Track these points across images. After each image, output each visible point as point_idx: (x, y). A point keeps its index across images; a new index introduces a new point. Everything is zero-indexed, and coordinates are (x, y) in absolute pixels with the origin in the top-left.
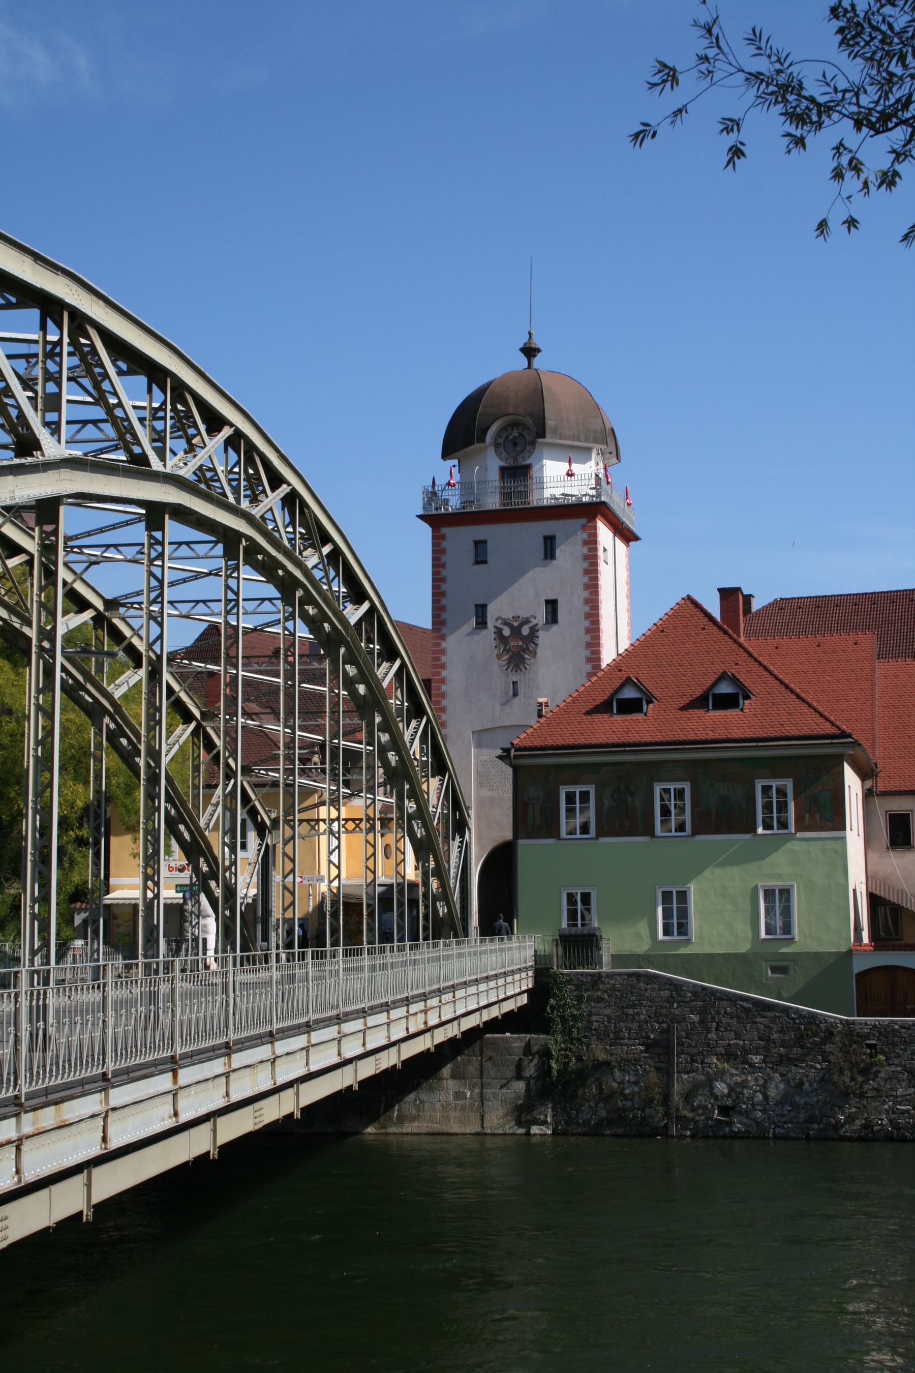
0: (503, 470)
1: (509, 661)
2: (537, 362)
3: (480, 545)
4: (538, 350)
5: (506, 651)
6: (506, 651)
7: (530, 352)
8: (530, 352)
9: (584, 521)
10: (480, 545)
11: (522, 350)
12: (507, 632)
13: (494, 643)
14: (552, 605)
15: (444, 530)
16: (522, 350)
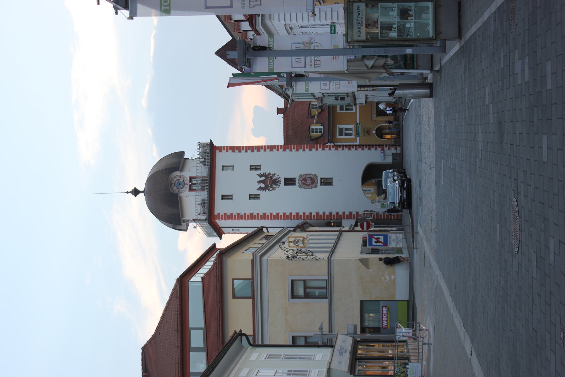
0: (191, 189)
1: (275, 184)
2: (141, 188)
3: (224, 197)
4: (135, 188)
5: (271, 187)
6: (271, 187)
7: (136, 192)
8: (136, 192)
9: (217, 152)
10: (224, 197)
11: (136, 196)
12: (263, 185)
13: (267, 191)
14: (252, 168)
15: (216, 214)
16: (136, 196)
